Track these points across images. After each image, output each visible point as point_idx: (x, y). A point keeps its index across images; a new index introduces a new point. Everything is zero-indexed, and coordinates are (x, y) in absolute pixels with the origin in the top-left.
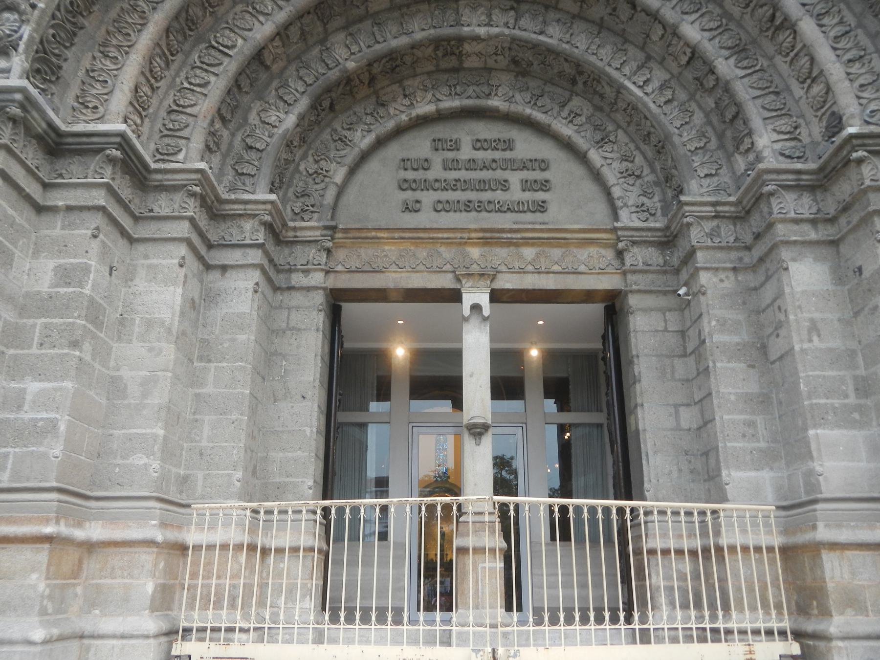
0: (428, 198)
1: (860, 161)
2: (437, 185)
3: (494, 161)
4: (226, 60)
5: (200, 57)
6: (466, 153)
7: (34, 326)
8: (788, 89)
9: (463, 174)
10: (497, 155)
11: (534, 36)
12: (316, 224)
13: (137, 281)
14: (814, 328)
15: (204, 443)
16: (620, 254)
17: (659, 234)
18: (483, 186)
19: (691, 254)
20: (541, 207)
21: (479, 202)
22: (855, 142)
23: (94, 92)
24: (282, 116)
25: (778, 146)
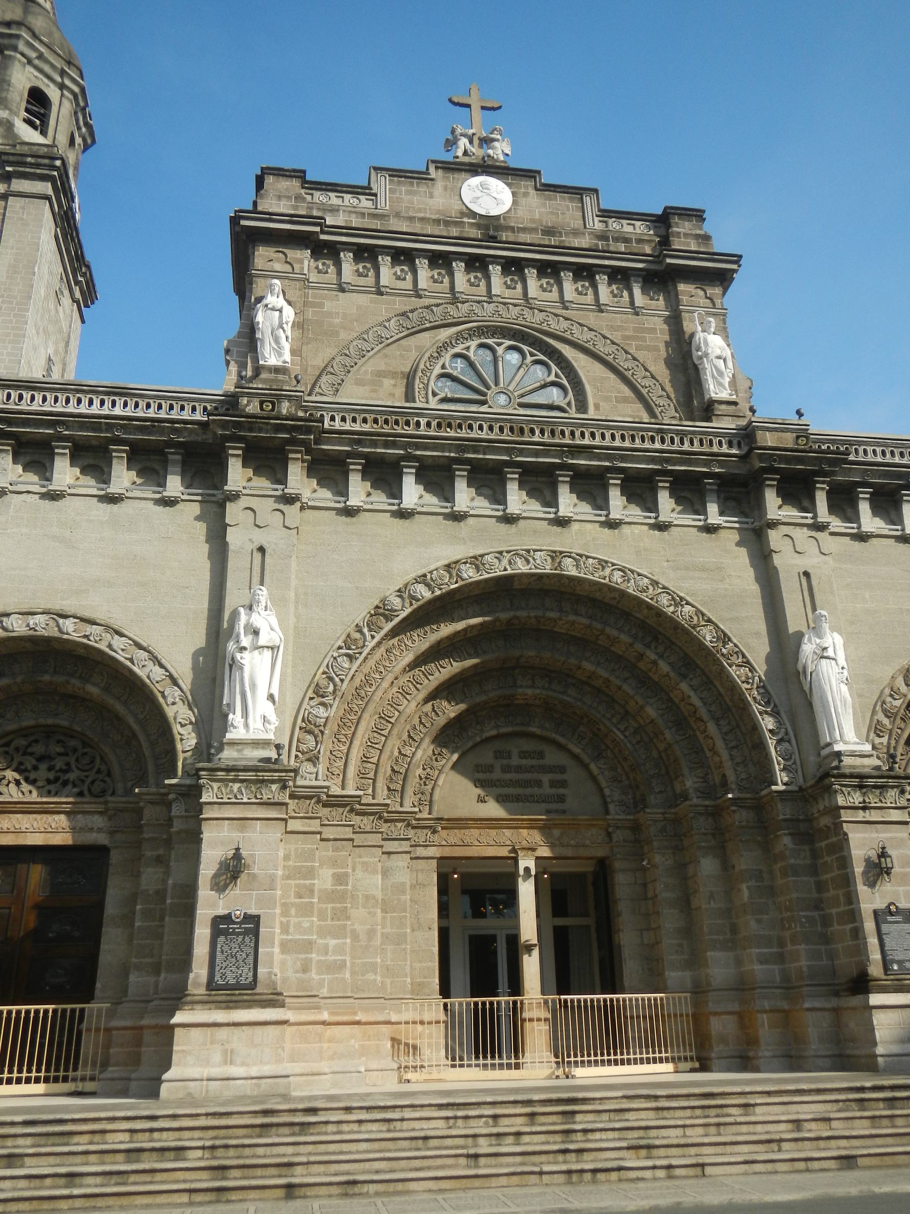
1: (734, 811)
2: (498, 783)
3: (532, 767)
4: (390, 725)
6: (515, 761)
7: (327, 908)
8: (703, 750)
10: (534, 762)
11: (560, 696)
13: (357, 871)
14: (712, 896)
15: (389, 963)
16: (609, 834)
18: (527, 784)
20: (561, 799)
23: (336, 765)
25: (696, 785)
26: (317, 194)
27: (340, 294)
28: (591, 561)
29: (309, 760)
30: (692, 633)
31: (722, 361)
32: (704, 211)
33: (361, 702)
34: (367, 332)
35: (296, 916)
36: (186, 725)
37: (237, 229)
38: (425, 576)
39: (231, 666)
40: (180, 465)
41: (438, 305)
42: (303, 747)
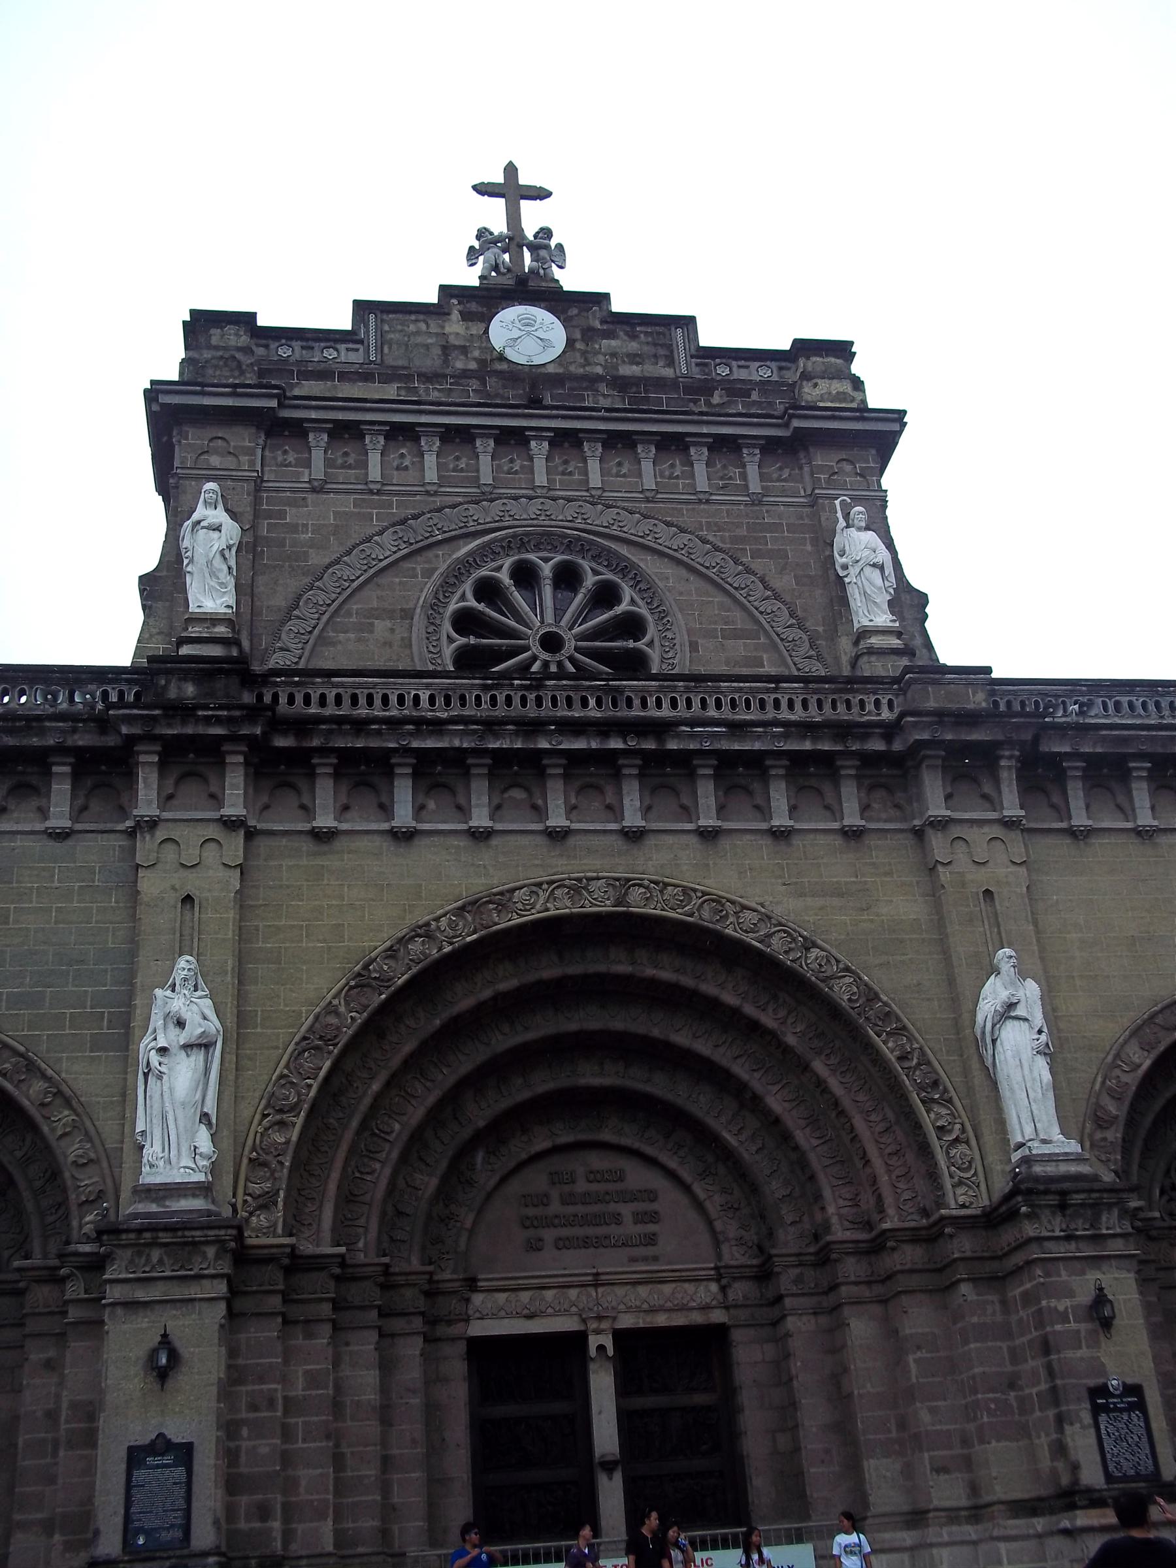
0: (549, 1235)
2: (556, 1221)
3: (607, 1193)
4: (387, 1146)
5: (365, 1145)
6: (581, 1186)
7: (297, 1423)
9: (580, 1209)
10: (611, 1187)
12: (455, 1277)
17: (755, 1270)
19: (779, 1299)
20: (651, 1240)
21: (597, 1238)
22: (888, 1234)
23: (307, 1210)
24: (426, 1179)
25: (844, 1211)
26: (273, 345)
27: (310, 497)
28: (669, 888)
29: (264, 1207)
30: (822, 990)
31: (878, 571)
32: (851, 343)
33: (341, 1115)
34: (349, 553)
35: (249, 1439)
36: (84, 1165)
37: (155, 408)
38: (428, 924)
39: (146, 1075)
40: (69, 781)
41: (454, 506)
42: (256, 1188)
